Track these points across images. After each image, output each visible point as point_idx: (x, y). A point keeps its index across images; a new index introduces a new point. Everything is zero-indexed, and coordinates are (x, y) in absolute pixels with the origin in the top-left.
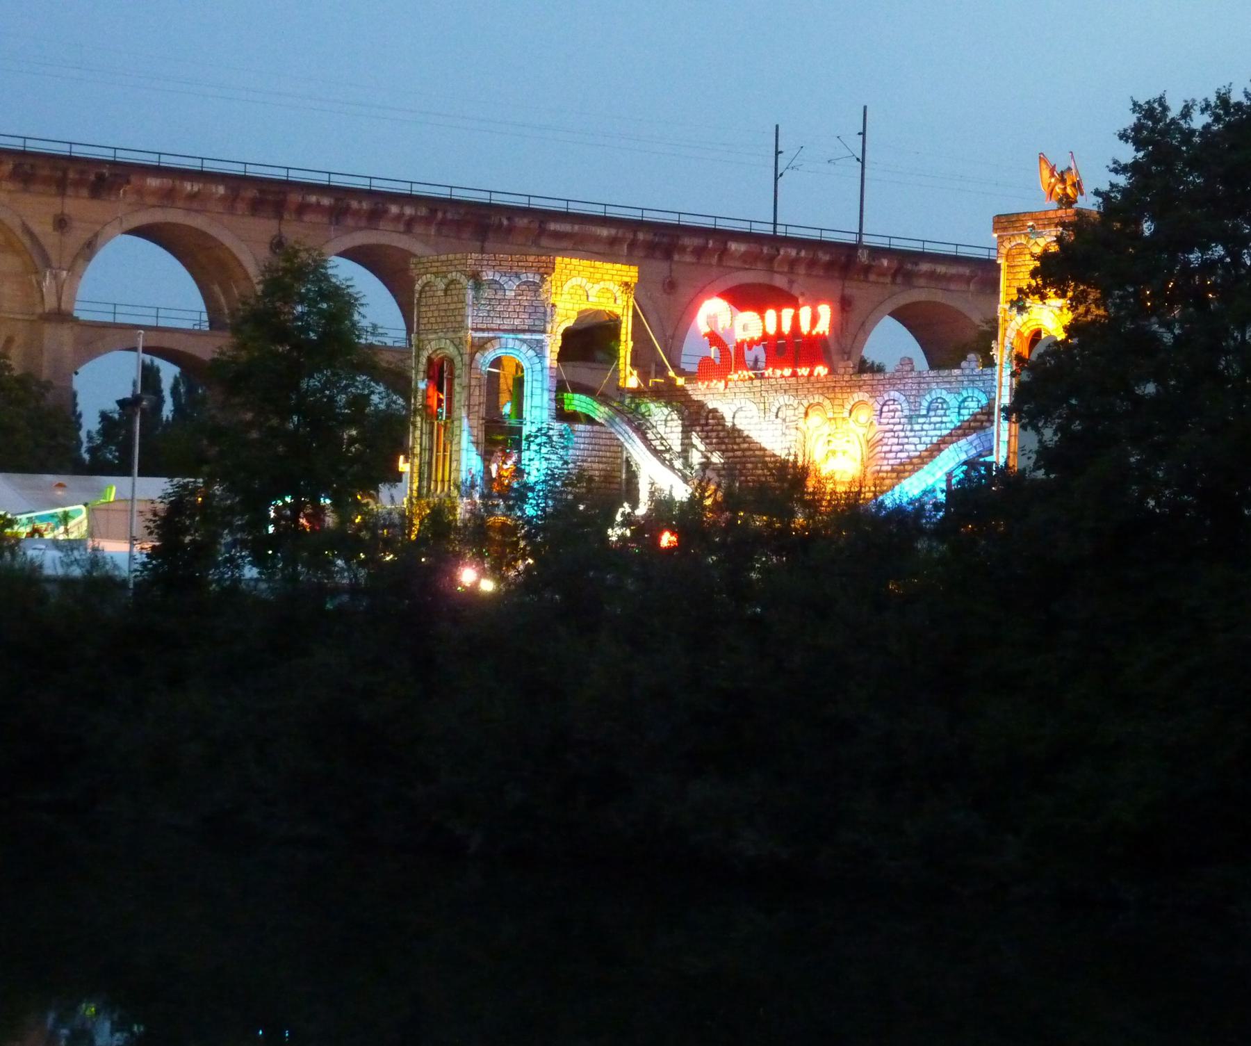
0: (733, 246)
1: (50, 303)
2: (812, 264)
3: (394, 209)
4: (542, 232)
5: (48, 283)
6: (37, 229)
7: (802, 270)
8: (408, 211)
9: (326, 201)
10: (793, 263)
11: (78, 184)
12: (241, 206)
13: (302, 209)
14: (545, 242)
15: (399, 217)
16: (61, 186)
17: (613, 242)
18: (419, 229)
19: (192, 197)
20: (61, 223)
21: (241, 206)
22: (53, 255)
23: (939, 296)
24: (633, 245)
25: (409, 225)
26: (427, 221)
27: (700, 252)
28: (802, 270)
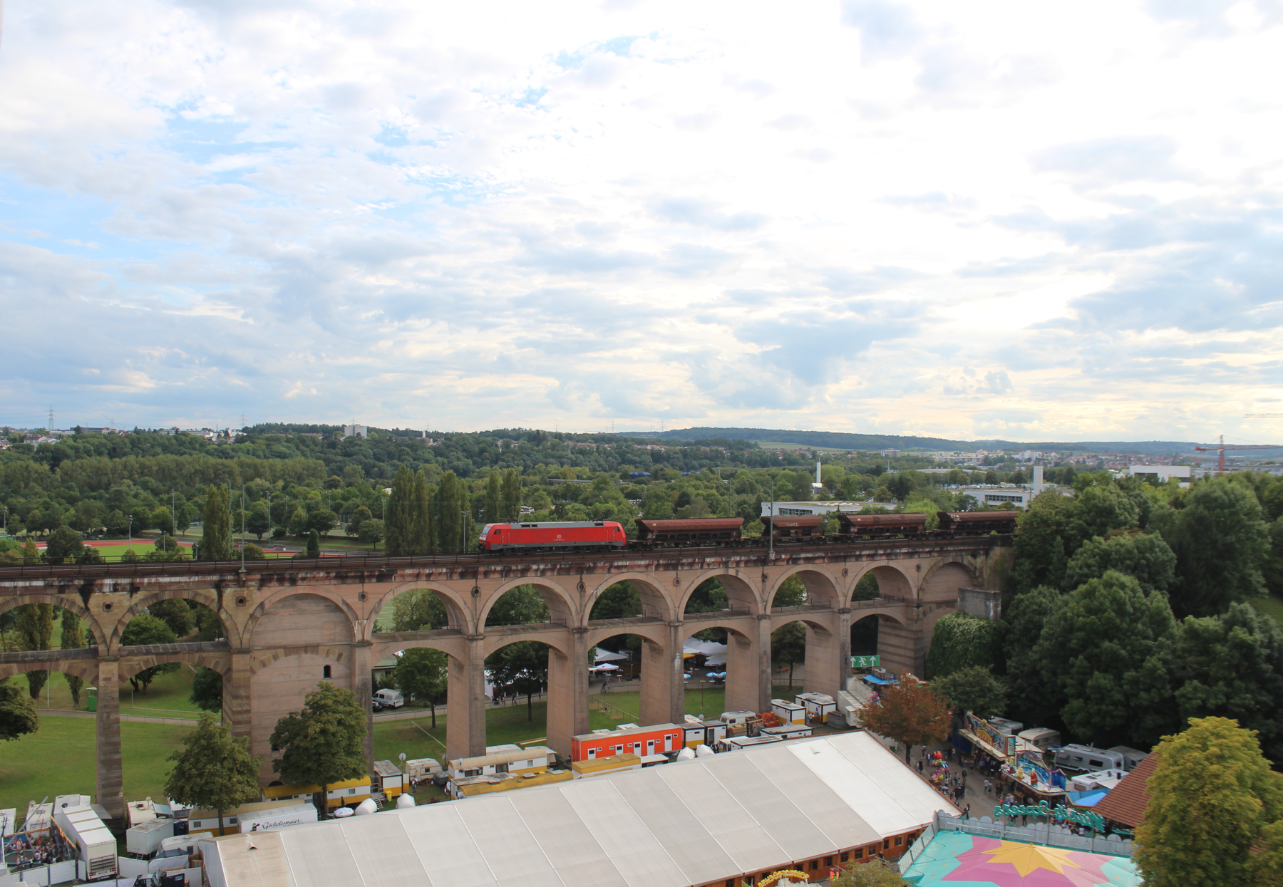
0: (708, 560)
1: (358, 637)
2: (747, 562)
3: (535, 567)
4: (611, 566)
5: (356, 628)
6: (348, 601)
7: (742, 565)
8: (542, 567)
9: (499, 568)
10: (738, 563)
11: (370, 577)
12: (456, 577)
13: (486, 574)
14: (613, 570)
15: (537, 570)
16: (362, 579)
17: (647, 566)
18: (549, 573)
19: (429, 575)
20: (363, 597)
21: (456, 577)
22: (359, 613)
23: (810, 567)
24: (658, 566)
25: (543, 572)
26: (552, 570)
27: (691, 565)
28: (742, 565)
